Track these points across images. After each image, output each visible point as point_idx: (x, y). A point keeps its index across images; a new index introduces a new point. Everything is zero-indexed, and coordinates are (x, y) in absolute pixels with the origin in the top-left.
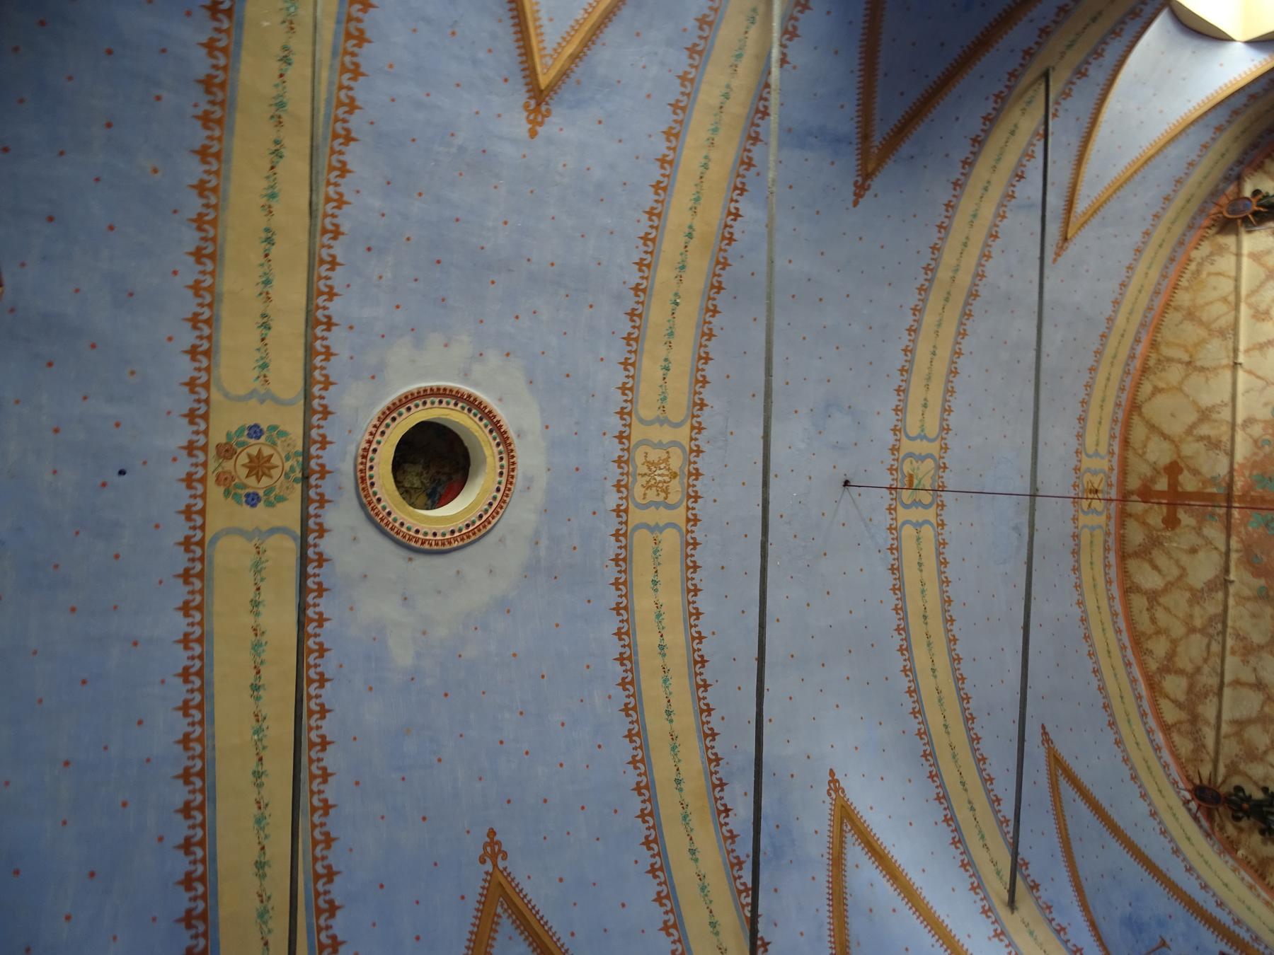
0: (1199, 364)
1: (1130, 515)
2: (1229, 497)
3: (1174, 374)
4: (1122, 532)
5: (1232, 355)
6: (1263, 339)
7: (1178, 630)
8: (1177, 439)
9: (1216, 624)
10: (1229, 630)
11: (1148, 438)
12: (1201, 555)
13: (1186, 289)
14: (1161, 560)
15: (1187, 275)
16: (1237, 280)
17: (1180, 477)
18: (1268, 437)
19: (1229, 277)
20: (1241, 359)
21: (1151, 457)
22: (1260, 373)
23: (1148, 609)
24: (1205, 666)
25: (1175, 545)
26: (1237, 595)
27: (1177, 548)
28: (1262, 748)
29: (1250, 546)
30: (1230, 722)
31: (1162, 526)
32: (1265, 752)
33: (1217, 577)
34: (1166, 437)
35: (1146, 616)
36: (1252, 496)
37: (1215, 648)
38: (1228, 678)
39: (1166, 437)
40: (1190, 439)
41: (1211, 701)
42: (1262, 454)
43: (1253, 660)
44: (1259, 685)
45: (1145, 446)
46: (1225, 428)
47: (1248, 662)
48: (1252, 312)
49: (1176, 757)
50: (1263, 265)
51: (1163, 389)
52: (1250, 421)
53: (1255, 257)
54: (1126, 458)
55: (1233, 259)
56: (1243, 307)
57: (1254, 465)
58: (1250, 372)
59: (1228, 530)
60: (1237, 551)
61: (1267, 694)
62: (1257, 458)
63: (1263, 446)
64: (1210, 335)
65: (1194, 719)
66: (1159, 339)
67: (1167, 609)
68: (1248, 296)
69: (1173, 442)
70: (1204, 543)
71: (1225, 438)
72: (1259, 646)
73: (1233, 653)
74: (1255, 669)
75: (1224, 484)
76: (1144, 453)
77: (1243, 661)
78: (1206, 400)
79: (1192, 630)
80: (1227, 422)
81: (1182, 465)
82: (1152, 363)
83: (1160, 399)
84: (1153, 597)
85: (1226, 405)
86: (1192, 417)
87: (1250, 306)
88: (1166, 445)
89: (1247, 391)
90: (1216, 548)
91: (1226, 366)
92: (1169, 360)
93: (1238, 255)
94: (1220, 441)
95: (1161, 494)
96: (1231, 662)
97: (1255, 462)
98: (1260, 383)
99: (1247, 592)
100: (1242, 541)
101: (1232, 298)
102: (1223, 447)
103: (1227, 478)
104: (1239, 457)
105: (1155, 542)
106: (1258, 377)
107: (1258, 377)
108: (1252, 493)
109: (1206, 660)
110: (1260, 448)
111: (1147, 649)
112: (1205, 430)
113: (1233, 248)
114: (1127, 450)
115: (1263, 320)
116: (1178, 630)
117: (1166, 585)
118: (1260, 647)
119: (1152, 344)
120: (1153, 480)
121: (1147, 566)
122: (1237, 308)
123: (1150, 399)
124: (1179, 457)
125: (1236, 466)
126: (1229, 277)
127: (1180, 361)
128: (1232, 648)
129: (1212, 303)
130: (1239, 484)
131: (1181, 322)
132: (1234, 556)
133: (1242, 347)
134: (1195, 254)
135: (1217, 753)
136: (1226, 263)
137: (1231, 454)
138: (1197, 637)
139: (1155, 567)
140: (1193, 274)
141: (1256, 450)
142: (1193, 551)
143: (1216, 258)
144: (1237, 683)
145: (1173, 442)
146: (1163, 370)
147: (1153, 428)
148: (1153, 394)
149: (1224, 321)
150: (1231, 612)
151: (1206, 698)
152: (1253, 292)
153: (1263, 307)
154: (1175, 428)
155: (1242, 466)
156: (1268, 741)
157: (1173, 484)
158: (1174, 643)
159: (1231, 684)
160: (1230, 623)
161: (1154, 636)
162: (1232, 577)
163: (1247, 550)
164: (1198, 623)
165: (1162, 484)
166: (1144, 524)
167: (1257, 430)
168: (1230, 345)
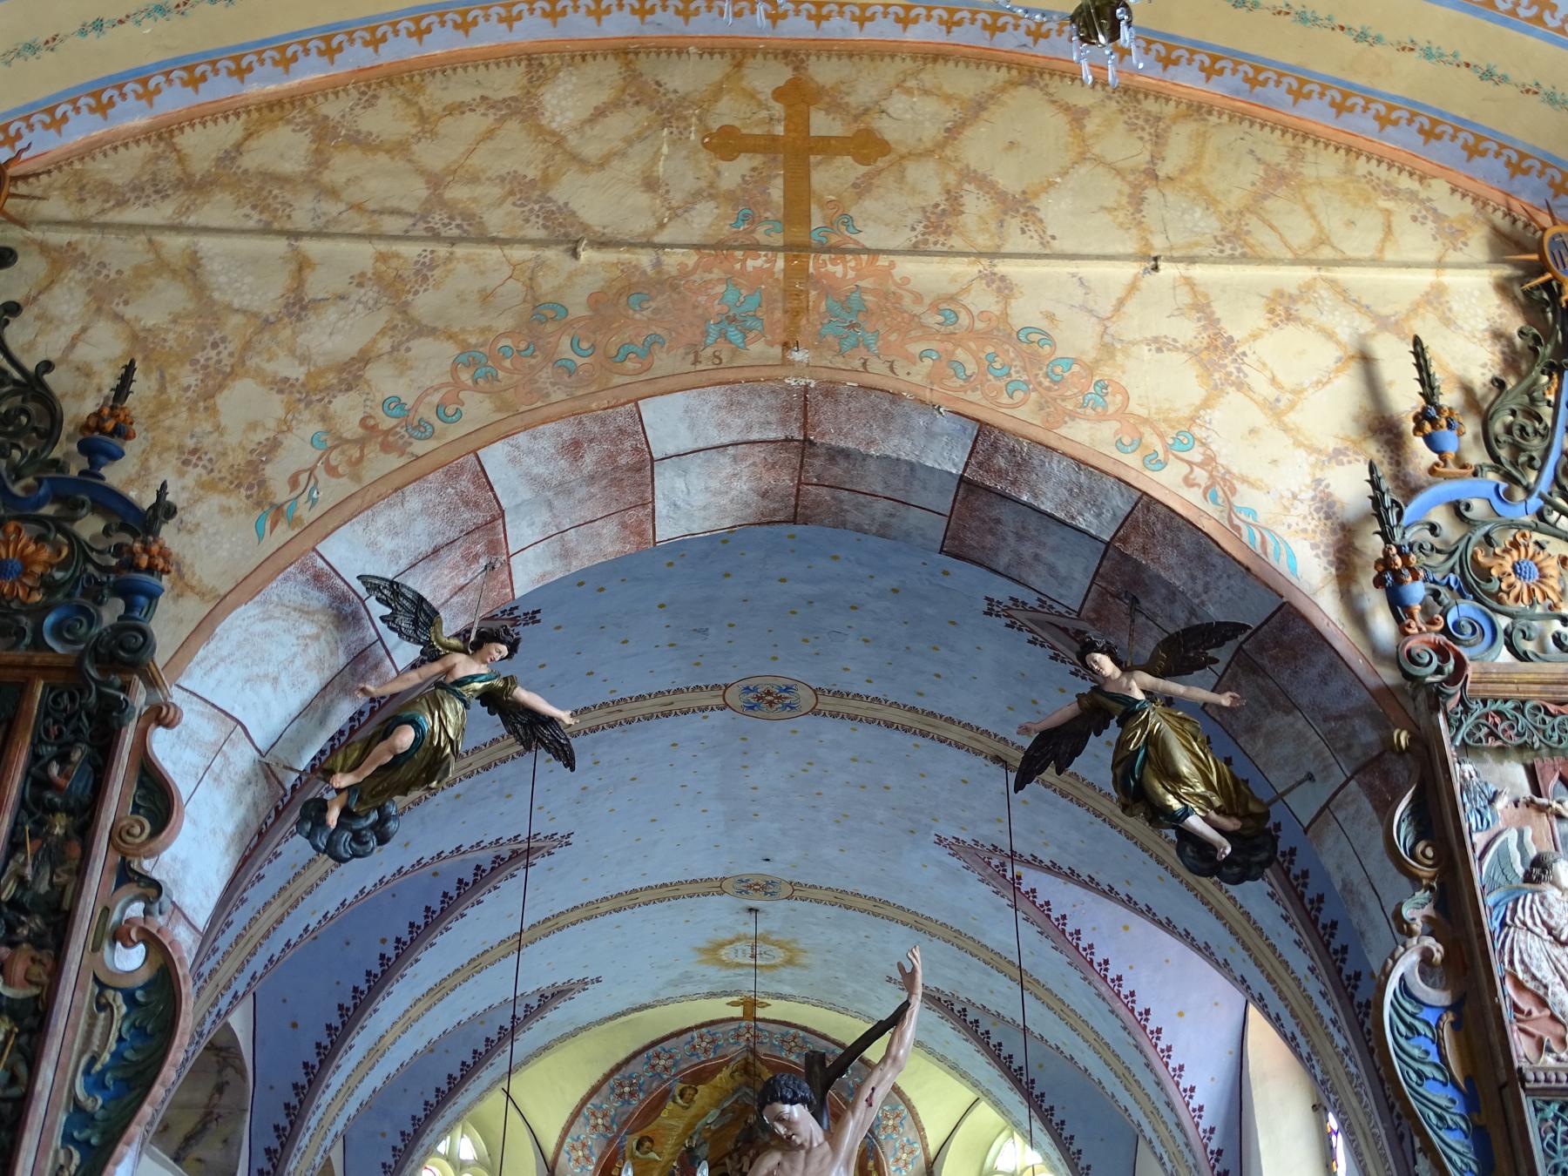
0: (1152, 194)
1: (739, 65)
3: (1127, 148)
4: (692, 49)
6: (1219, 310)
7: (433, 156)
8: (948, 152)
9: (458, 226)
10: (442, 250)
11: (948, 98)
12: (643, 199)
13: (1348, 171)
14: (619, 125)
15: (1382, 172)
18: (964, 319)
19: (1381, 250)
21: (898, 104)
22: (1130, 307)
23: (483, 98)
24: (342, 207)
25: (665, 150)
26: (540, 264)
27: (657, 153)
28: (129, 312)
29: (674, 288)
30: (196, 252)
31: (715, 126)
32: (118, 317)
33: (585, 227)
34: (953, 132)
35: (468, 95)
37: (392, 224)
38: (312, 247)
39: (953, 132)
40: (951, 178)
41: (247, 216)
42: (918, 310)
43: (369, 293)
44: (298, 306)
45: (926, 92)
46: (983, 241)
47: (360, 285)
49: (89, 151)
51: (1082, 127)
54: (893, 57)
56: (1305, 273)
58: (1133, 287)
59: (717, 247)
60: (658, 264)
61: (281, 319)
62: (907, 301)
63: (940, 312)
64: (1229, 213)
65: (194, 186)
66: (1213, 119)
67: (489, 135)
68: (1333, 283)
69: (942, 145)
70: (674, 204)
71: (956, 242)
72: (407, 304)
73: (383, 257)
74: (342, 298)
76: (909, 92)
77: (363, 274)
78: (1055, 209)
79: (436, 182)
80: (999, 247)
81: (881, 163)
82: (1150, 105)
83: (1056, 123)
84: (523, 109)
86: (1008, 178)
87: (1308, 287)
88: (931, 132)
90: (661, 226)
91: (1148, 244)
92: (1159, 139)
94: (948, 233)
95: (798, 121)
96: (363, 254)
97: (901, 297)
98: (1105, 308)
99: (547, 283)
100: (685, 273)
101: (1326, 253)
102: (931, 239)
104: (908, 267)
105: (670, 113)
106: (1121, 302)
107: (1121, 302)
108: (813, 293)
109: (358, 207)
110: (935, 307)
111: (375, 97)
112: (975, 205)
114: (914, 59)
115: (1272, 311)
116: (433, 156)
117: (553, 133)
118: (404, 310)
119: (1200, 107)
120: (836, 108)
121: (603, 96)
123: (1054, 102)
124: (902, 157)
125: (883, 261)
128: (397, 256)
129: (1313, 217)
132: (645, 259)
133: (1198, 272)
134: (1439, 188)
135: (104, 227)
136: (1416, 240)
138: (421, 190)
139: (600, 113)
140: (1387, 183)
141: (927, 301)
142: (650, 184)
143: (1430, 224)
144: (302, 265)
145: (942, 145)
146: (1132, 128)
147: (977, 108)
148: (1067, 109)
149: (1262, 237)
150: (495, 253)
151: (254, 207)
153: (1304, 310)
154: (977, 148)
156: (150, 323)
157: (828, 147)
158: (400, 148)
159: (296, 250)
160: (461, 250)
161: (415, 110)
162: (586, 254)
163: (664, 283)
164: (457, 193)
165: (822, 124)
166: (718, 92)
167: (982, 301)
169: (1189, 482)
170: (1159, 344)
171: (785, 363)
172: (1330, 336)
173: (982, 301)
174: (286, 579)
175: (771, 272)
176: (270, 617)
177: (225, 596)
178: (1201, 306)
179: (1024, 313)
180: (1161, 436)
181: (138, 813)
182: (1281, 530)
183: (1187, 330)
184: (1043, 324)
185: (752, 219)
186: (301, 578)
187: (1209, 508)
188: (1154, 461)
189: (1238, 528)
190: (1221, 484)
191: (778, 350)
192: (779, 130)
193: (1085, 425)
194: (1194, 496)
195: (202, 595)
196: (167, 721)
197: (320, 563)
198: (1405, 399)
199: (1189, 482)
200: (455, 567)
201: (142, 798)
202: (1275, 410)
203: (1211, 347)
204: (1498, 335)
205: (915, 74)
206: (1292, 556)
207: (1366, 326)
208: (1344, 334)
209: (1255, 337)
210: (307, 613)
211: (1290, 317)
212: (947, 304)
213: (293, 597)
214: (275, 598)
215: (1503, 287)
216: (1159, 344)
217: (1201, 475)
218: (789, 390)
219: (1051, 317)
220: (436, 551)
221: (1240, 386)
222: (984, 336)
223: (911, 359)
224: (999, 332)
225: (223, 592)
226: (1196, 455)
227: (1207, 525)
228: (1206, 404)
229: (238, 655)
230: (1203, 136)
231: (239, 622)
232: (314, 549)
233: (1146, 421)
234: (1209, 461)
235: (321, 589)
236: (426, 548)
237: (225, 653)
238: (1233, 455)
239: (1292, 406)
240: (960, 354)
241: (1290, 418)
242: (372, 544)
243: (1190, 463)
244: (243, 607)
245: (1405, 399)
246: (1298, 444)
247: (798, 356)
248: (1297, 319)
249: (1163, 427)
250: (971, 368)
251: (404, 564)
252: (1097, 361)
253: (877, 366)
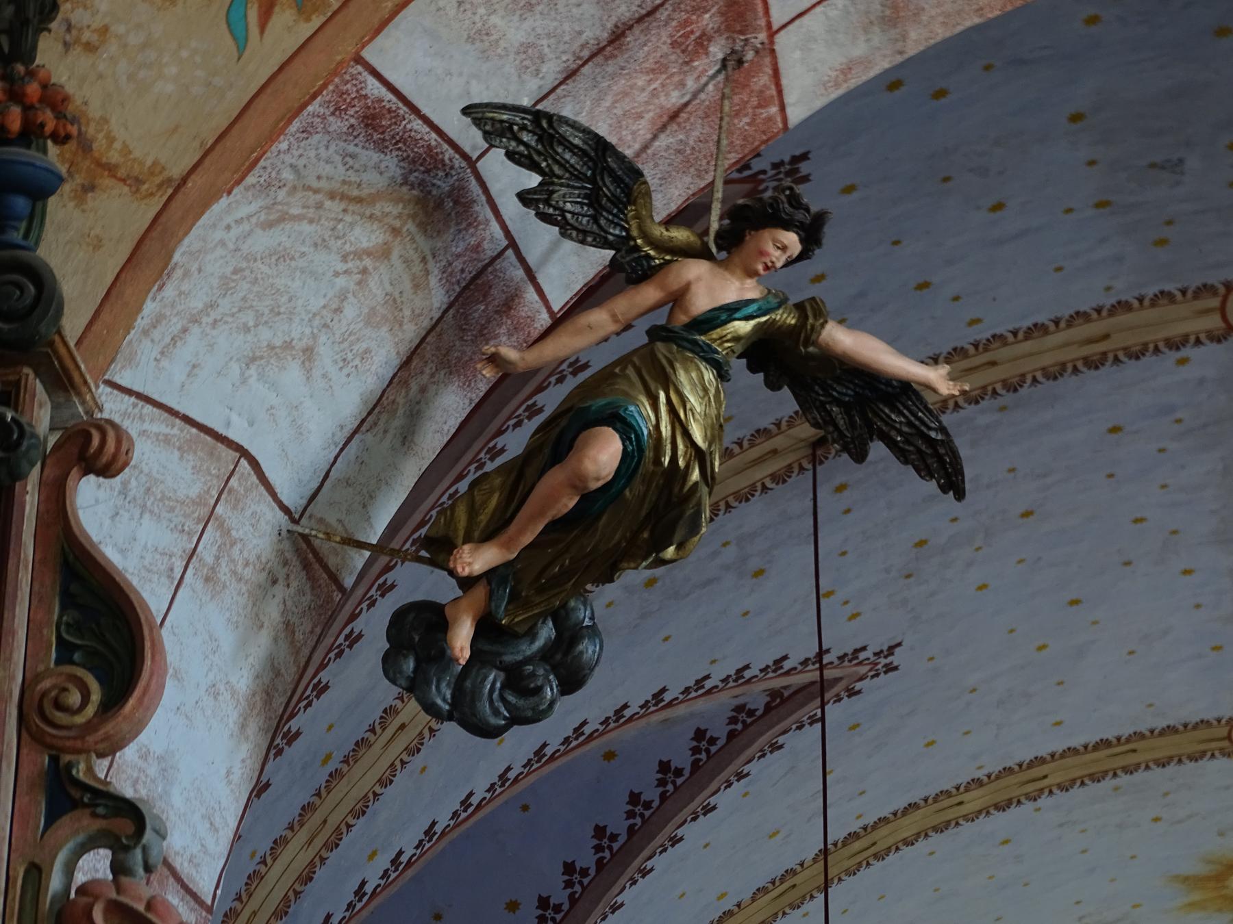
174: (306, 131)
176: (283, 218)
177: (184, 180)
181: (72, 663)
186: (336, 124)
195: (135, 182)
196: (104, 459)
197: (373, 88)
200: (660, 68)
201: (76, 628)
210: (359, 200)
213: (327, 169)
214: (287, 175)
220: (618, 36)
225: (177, 171)
229: (225, 305)
231: (219, 234)
232: (359, 60)
235: (381, 147)
236: (595, 33)
237: (197, 304)
242: (480, 35)
244: (224, 201)
251: (552, 70)
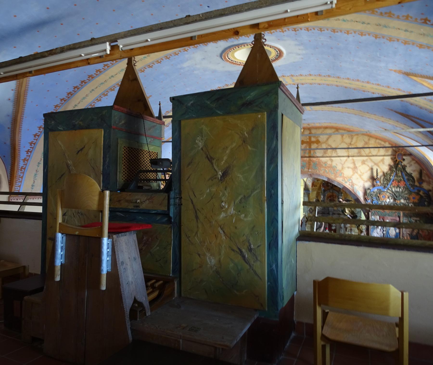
2: (310, 157)
5: (352, 155)
6: (356, 163)
8: (327, 142)
16: (376, 156)
17: (315, 144)
20: (350, 158)
22: (346, 163)
34: (328, 139)
36: (310, 162)
46: (330, 155)
48: (365, 160)
50: (380, 162)
52: (332, 161)
53: (383, 161)
55: (383, 154)
56: (366, 158)
57: (319, 162)
58: (346, 160)
71: (327, 155)
75: (314, 155)
81: (319, 144)
85: (337, 154)
87: (367, 160)
88: (325, 139)
89: (341, 160)
91: (349, 154)
92: (352, 139)
93: (384, 156)
94: (326, 154)
95: (310, 138)
98: (343, 163)
101: (370, 154)
103: (316, 156)
106: (345, 162)
107: (345, 162)
108: (311, 162)
113: (387, 154)
115: (362, 163)
122: (367, 156)
125: (319, 158)
126: (377, 153)
127: (351, 141)
130: (314, 159)
131: (364, 141)
133: (354, 158)
137: (322, 157)
145: (326, 141)
152: (371, 160)
153: (366, 163)
155: (319, 159)
157: (313, 142)
165: (313, 139)
167: (329, 162)
168: (355, 155)
169: (349, 185)
170: (348, 168)
171: (309, 171)
172: (368, 166)
173: (329, 162)
175: (307, 160)
178: (354, 163)
179: (334, 164)
180: (347, 179)
182: (359, 190)
183: (352, 166)
184: (335, 165)
185: (305, 153)
187: (351, 188)
188: (346, 182)
189: (354, 190)
190: (353, 185)
191: (307, 170)
192: (308, 140)
193: (339, 178)
194: (350, 186)
198: (375, 174)
199: (349, 185)
202: (360, 176)
203: (354, 168)
204: (390, 165)
205: (323, 131)
206: (359, 193)
207: (373, 164)
208: (370, 166)
209: (359, 166)
211: (364, 164)
212: (325, 163)
215: (392, 159)
216: (348, 168)
217: (351, 184)
218: (309, 174)
219: (337, 164)
221: (357, 173)
222: (329, 167)
223: (321, 170)
224: (331, 167)
226: (351, 181)
227: (351, 190)
228: (353, 175)
230: (357, 138)
233: (346, 177)
234: (352, 182)
238: (354, 182)
239: (362, 175)
240: (327, 170)
241: (362, 177)
243: (350, 182)
245: (375, 174)
246: (362, 180)
247: (310, 170)
248: (365, 164)
249: (348, 178)
250: (328, 171)
252: (341, 170)
253: (318, 171)
